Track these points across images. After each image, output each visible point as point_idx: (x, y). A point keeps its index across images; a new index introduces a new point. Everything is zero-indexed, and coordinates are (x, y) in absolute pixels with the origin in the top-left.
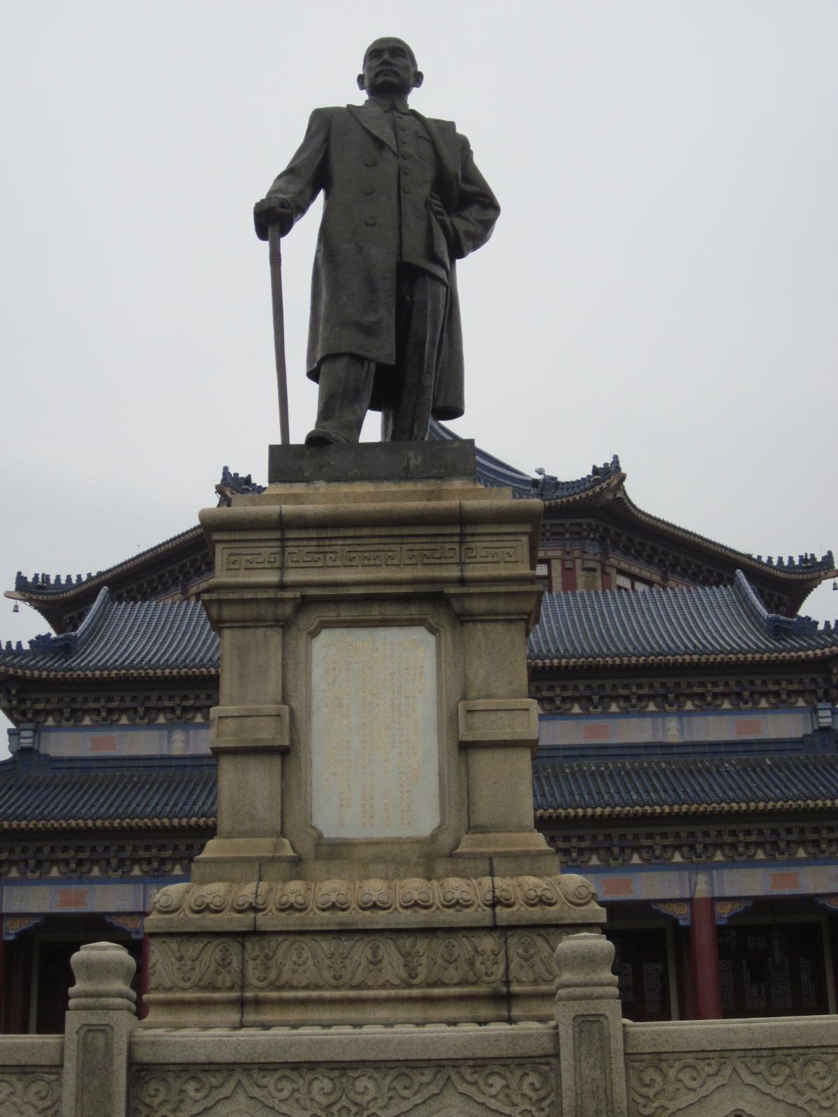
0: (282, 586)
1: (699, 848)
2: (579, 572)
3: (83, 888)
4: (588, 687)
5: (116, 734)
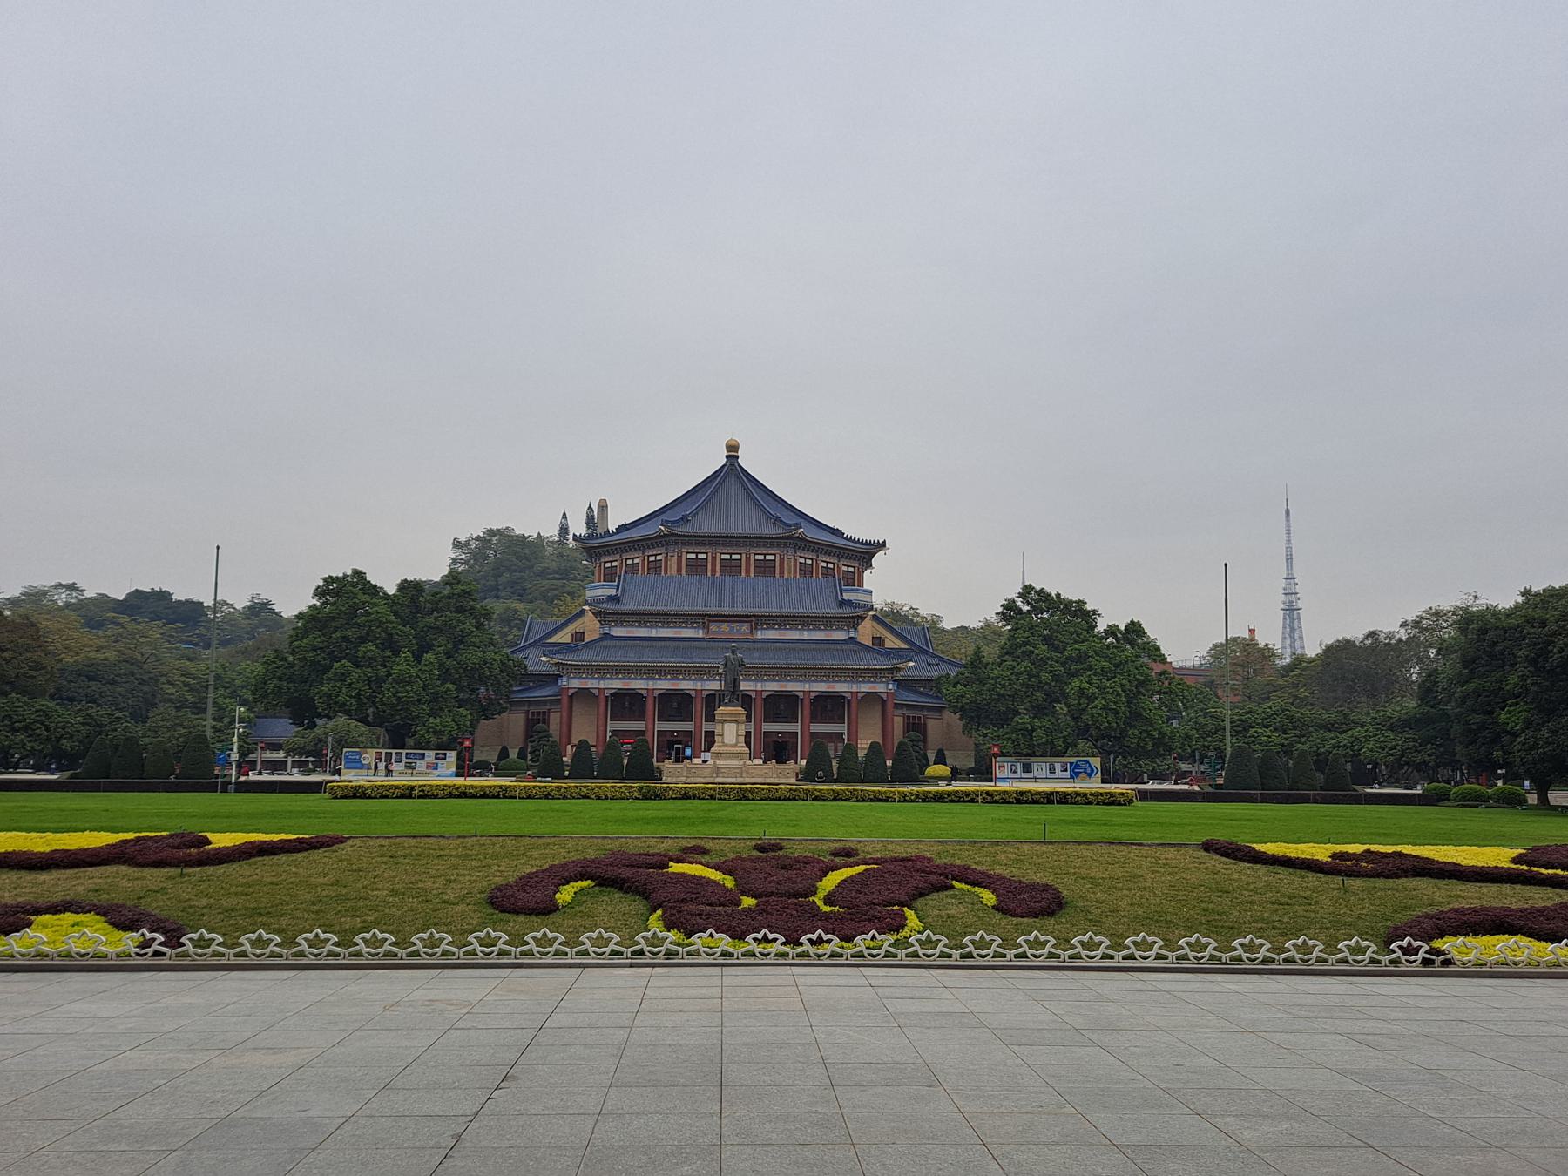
5: (635, 629)
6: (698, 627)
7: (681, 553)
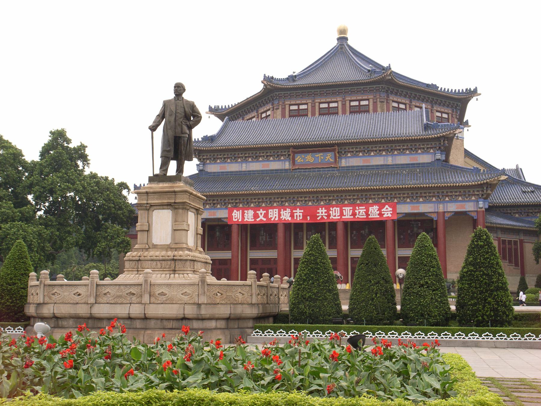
0: (147, 204)
1: (389, 198)
2: (378, 103)
3: (215, 211)
4: (364, 147)
5: (226, 165)
6: (284, 160)
7: (285, 105)
